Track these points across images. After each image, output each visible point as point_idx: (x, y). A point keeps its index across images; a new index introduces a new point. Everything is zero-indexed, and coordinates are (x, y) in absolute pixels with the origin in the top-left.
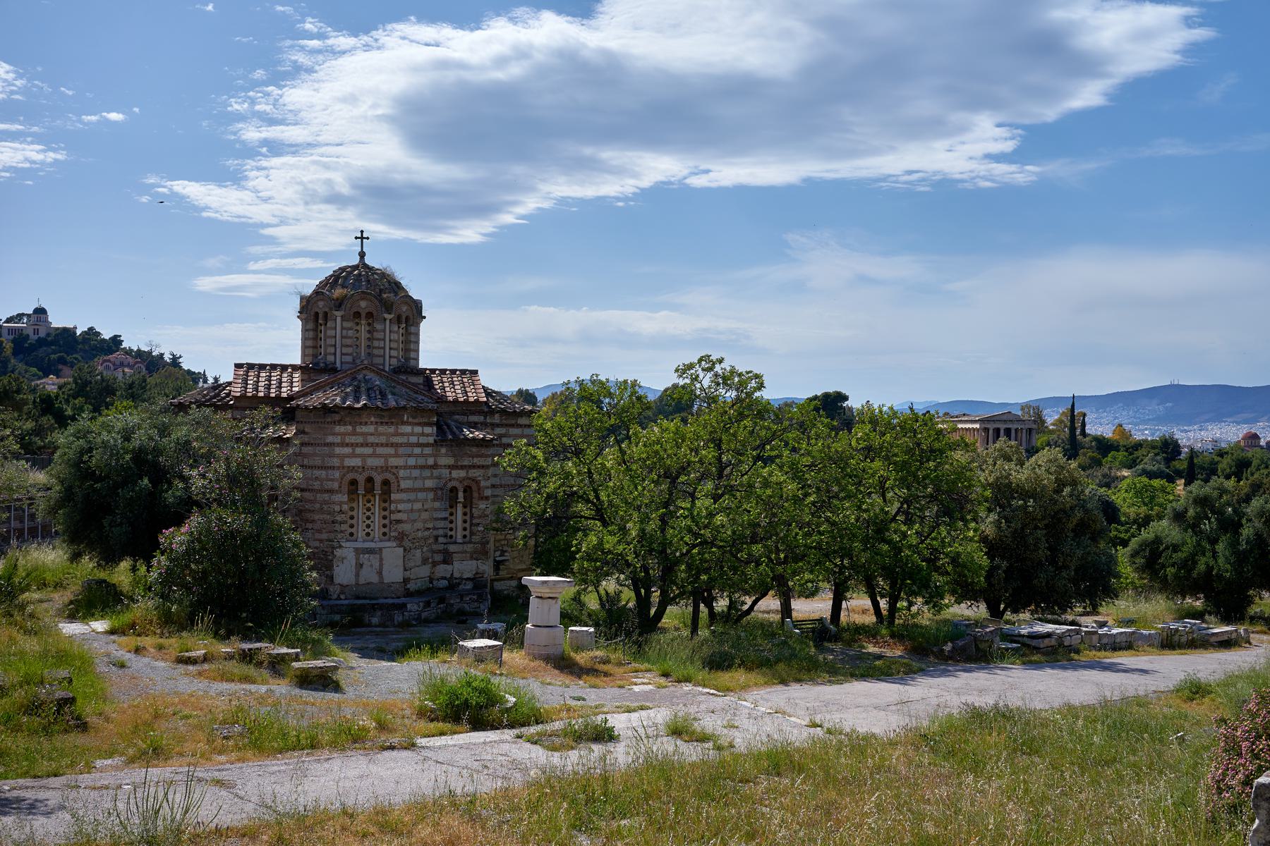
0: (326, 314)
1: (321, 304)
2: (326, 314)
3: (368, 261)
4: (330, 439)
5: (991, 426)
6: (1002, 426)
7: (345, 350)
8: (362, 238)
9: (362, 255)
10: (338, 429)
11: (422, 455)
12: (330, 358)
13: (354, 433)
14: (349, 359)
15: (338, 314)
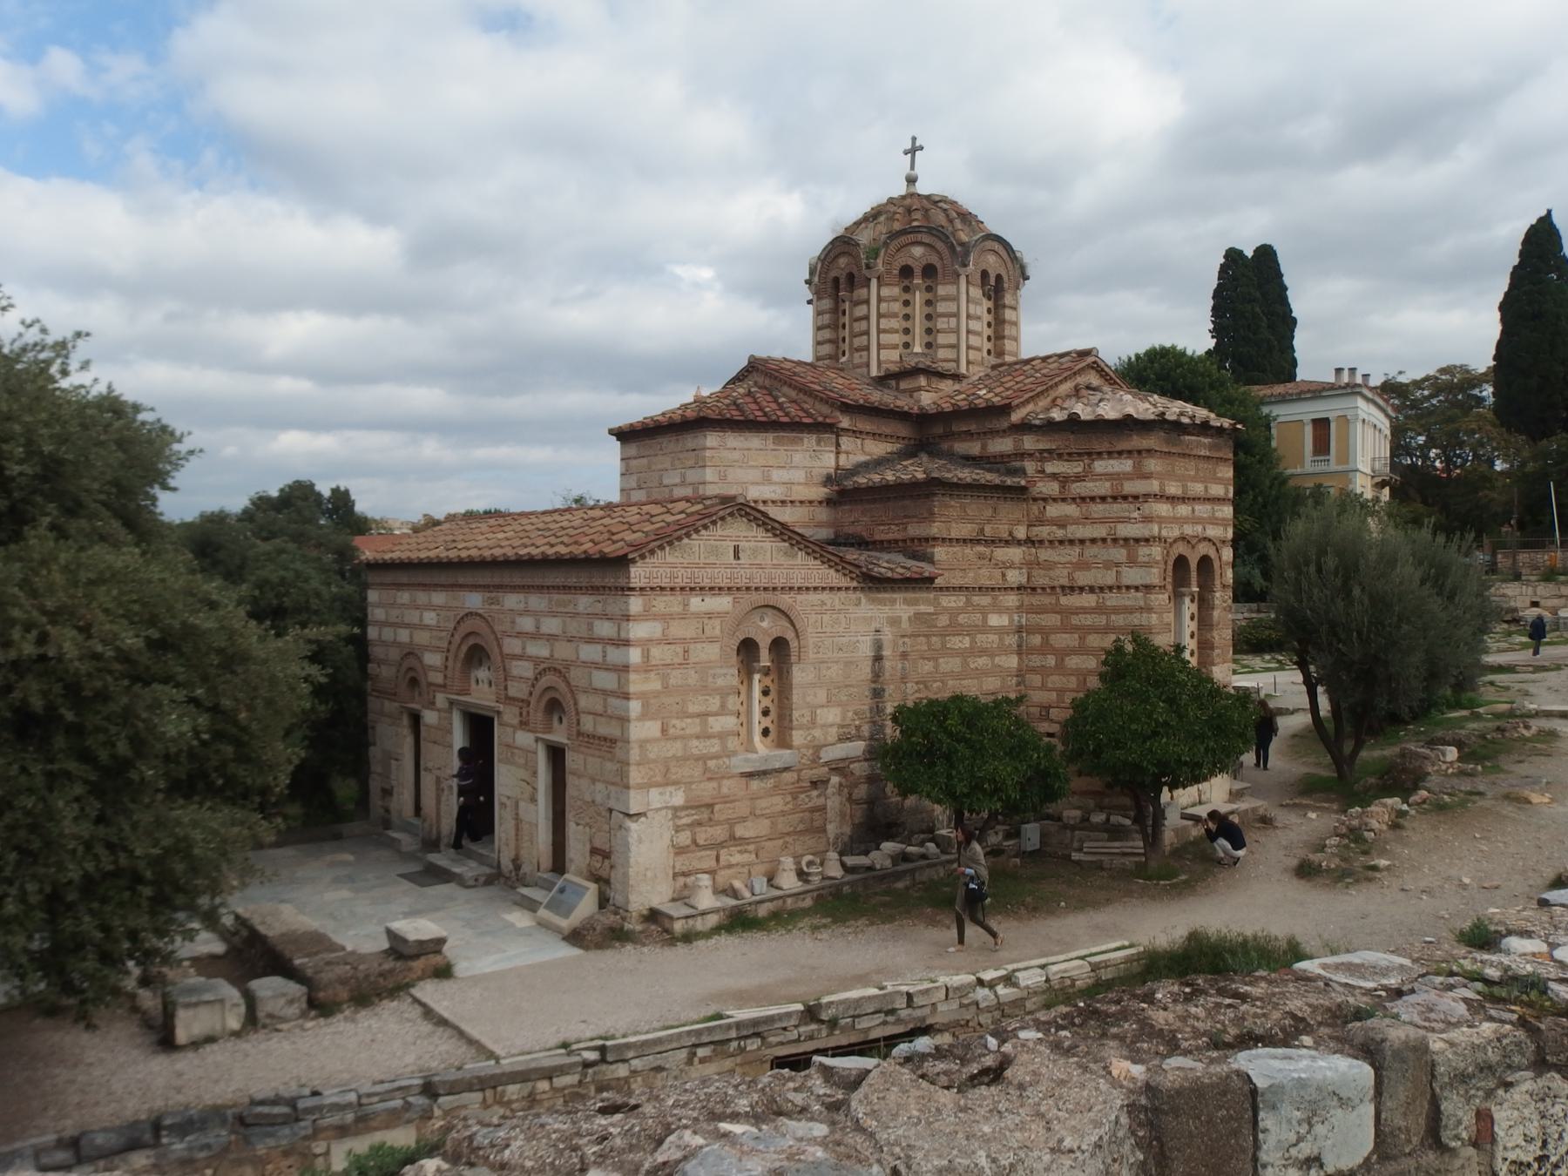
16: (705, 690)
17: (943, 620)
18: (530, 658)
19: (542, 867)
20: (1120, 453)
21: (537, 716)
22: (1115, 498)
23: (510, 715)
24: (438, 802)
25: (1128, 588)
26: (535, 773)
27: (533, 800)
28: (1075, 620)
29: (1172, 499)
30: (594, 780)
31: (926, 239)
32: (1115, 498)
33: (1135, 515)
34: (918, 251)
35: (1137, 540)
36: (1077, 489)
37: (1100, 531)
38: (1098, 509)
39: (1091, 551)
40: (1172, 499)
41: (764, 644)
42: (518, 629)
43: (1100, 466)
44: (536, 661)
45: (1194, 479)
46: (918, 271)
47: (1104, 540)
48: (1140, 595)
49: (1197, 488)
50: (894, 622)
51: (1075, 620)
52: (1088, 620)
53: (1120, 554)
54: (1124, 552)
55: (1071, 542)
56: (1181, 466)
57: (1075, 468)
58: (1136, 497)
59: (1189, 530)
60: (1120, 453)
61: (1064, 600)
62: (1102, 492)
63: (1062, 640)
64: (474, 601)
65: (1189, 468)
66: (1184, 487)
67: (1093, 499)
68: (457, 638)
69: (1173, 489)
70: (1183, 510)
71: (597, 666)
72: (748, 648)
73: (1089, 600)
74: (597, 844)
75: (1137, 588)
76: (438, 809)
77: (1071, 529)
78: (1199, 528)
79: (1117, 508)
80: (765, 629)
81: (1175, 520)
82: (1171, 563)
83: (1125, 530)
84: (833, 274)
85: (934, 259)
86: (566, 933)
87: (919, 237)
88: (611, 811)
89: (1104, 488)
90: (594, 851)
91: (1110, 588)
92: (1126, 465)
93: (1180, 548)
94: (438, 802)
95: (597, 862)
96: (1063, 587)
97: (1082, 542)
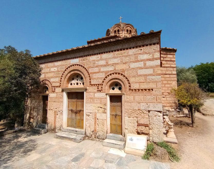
18: (102, 72)
19: (108, 133)
20: (171, 54)
21: (106, 87)
22: (170, 61)
23: (90, 89)
24: (55, 118)
25: (173, 74)
26: (105, 105)
27: (105, 112)
28: (166, 79)
30: (139, 103)
31: (130, 26)
32: (170, 61)
33: (173, 63)
34: (129, 28)
35: (174, 67)
36: (165, 59)
37: (169, 66)
38: (168, 62)
39: (168, 68)
42: (96, 65)
43: (168, 56)
44: (106, 72)
46: (129, 31)
47: (169, 67)
48: (175, 75)
51: (166, 79)
52: (168, 79)
53: (172, 69)
54: (172, 69)
55: (165, 67)
57: (165, 56)
58: (173, 61)
60: (171, 54)
61: (165, 76)
62: (169, 60)
63: (165, 82)
64: (76, 61)
67: (167, 61)
68: (66, 72)
71: (141, 68)
73: (168, 76)
74: (142, 122)
75: (174, 74)
76: (55, 121)
77: (165, 65)
79: (171, 62)
83: (172, 66)
84: (114, 30)
85: (131, 29)
86: (143, 153)
87: (129, 26)
88: (149, 111)
89: (169, 59)
90: (139, 125)
91: (171, 74)
92: (172, 56)
94: (55, 118)
95: (143, 129)
96: (164, 74)
97: (166, 67)
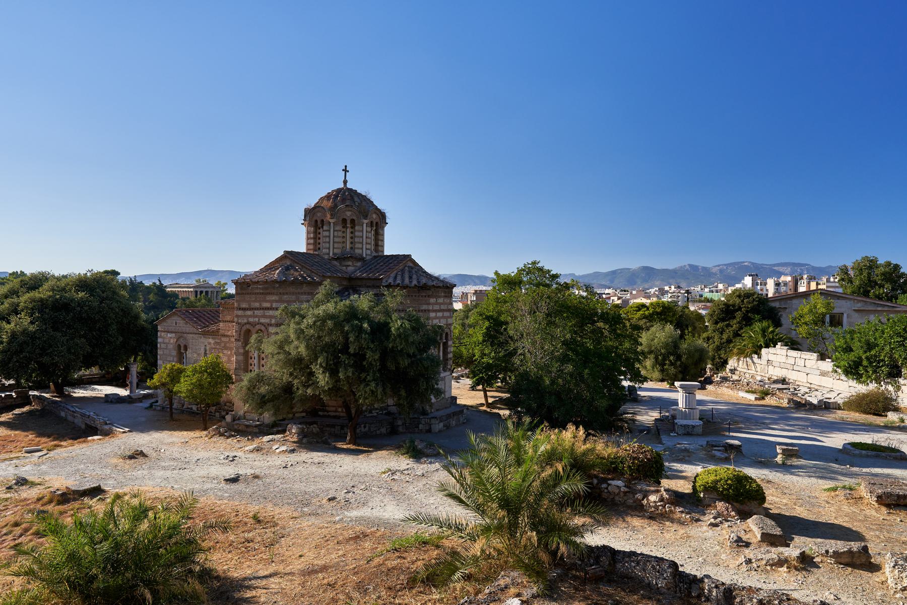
0: (353, 221)
1: (349, 214)
2: (353, 221)
3: (349, 186)
4: (424, 307)
5: (199, 290)
6: (204, 290)
7: (368, 247)
8: (346, 171)
9: (345, 182)
10: (432, 300)
11: (443, 317)
12: (360, 251)
13: (436, 304)
14: (369, 252)
15: (365, 221)
16: (170, 355)
17: (223, 345)
29: (244, 309)
40: (244, 309)
41: (182, 346)
45: (255, 301)
49: (257, 305)
50: (210, 343)
56: (247, 297)
59: (251, 320)
65: (253, 297)
66: (250, 305)
69: (244, 305)
70: (249, 313)
72: (179, 346)
78: (257, 319)
80: (182, 342)
81: (245, 316)
82: (242, 333)
93: (248, 326)
